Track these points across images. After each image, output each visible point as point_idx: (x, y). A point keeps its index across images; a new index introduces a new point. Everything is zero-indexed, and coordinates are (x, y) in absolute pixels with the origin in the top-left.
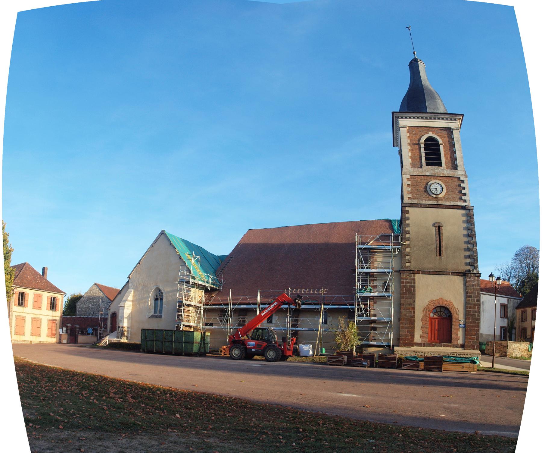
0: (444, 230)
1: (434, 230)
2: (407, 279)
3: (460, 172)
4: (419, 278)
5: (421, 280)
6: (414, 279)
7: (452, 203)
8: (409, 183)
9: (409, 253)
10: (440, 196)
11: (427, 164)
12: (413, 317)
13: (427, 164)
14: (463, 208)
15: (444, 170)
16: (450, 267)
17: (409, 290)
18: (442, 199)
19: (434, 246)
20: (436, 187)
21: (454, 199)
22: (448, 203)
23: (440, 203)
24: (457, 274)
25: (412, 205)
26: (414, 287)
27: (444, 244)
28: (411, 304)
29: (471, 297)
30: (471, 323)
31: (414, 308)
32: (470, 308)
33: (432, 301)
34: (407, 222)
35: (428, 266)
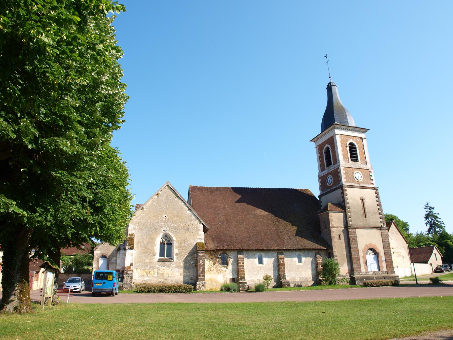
0: (365, 201)
1: (360, 202)
2: (352, 232)
3: (368, 166)
4: (357, 230)
5: (359, 232)
6: (355, 232)
7: (367, 186)
8: (344, 172)
9: (350, 216)
10: (360, 181)
11: (352, 160)
12: (359, 255)
13: (352, 160)
14: (374, 188)
15: (359, 164)
16: (372, 224)
17: (354, 239)
18: (361, 182)
19: (362, 212)
20: (359, 175)
21: (367, 183)
22: (365, 185)
23: (361, 185)
24: (376, 228)
25: (348, 186)
26: (356, 237)
27: (366, 210)
28: (356, 248)
29: (385, 242)
30: (388, 257)
31: (358, 250)
32: (386, 248)
33: (366, 245)
34: (347, 197)
35: (361, 224)
